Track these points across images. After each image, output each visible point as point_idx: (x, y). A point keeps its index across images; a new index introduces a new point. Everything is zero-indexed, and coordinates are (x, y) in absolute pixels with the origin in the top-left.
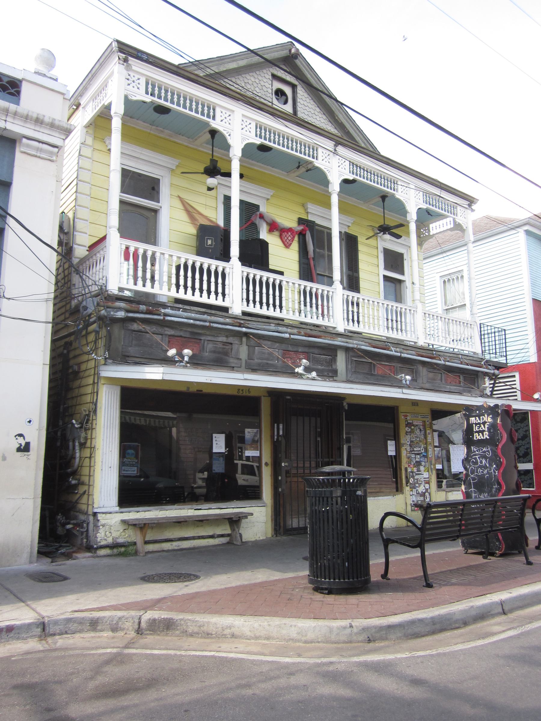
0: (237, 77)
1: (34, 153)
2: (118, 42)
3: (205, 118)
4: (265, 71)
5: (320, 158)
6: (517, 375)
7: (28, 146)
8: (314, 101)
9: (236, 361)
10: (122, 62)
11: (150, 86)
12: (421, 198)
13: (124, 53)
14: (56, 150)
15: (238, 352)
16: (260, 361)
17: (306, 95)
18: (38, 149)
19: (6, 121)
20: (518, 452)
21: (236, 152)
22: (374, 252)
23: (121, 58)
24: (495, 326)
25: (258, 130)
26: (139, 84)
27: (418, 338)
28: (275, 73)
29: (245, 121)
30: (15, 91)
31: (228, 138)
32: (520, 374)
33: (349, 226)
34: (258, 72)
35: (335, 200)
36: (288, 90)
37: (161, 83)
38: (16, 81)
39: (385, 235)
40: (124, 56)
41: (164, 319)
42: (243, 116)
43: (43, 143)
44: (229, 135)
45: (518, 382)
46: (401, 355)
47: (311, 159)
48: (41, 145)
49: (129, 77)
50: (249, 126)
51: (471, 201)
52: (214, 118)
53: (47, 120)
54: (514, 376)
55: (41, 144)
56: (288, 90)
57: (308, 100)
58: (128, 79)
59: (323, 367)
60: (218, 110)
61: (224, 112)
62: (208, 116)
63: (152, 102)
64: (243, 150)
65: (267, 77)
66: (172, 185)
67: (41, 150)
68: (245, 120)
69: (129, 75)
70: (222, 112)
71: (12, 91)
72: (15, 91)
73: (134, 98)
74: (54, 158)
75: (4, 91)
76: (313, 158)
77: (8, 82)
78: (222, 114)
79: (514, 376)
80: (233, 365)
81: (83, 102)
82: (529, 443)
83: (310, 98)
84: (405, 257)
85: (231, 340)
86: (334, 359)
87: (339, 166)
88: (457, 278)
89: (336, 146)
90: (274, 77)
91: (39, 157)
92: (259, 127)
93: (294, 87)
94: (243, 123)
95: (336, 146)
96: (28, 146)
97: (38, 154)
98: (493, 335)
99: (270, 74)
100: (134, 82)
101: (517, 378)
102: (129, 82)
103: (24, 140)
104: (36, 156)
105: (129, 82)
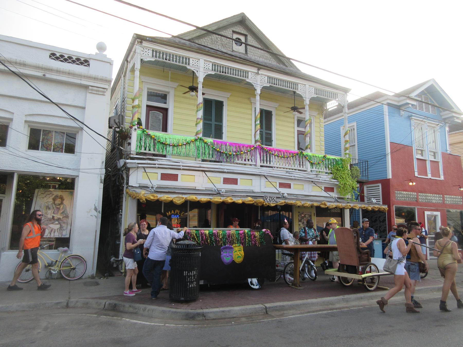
0: (212, 35)
1: (96, 92)
2: (136, 34)
3: (184, 65)
4: (228, 30)
5: (250, 77)
6: (380, 185)
7: (92, 90)
8: (258, 42)
10: (139, 43)
11: (154, 53)
12: (313, 92)
13: (140, 39)
14: (106, 90)
17: (253, 39)
18: (97, 91)
19: (81, 80)
20: (380, 229)
21: (201, 79)
22: (292, 120)
23: (138, 41)
25: (214, 67)
26: (149, 52)
27: (307, 168)
28: (235, 30)
29: (206, 63)
30: (87, 64)
31: (196, 73)
33: (276, 108)
34: (224, 31)
37: (160, 51)
38: (87, 59)
39: (294, 112)
40: (140, 40)
42: (205, 60)
43: (99, 87)
44: (197, 72)
45: (381, 190)
47: (244, 78)
48: (98, 89)
49: (144, 50)
50: (208, 66)
51: (346, 91)
52: (189, 64)
53: (99, 77)
54: (379, 186)
55: (98, 88)
56: (243, 39)
58: (143, 51)
60: (191, 60)
61: (194, 60)
62: (186, 64)
63: (155, 61)
64: (205, 79)
65: (230, 33)
66: (175, 96)
67: (99, 91)
69: (144, 49)
70: (193, 60)
71: (86, 64)
72: (87, 64)
73: (146, 60)
75: (82, 65)
76: (246, 77)
77: (83, 61)
78: (193, 62)
81: (129, 60)
82: (386, 224)
83: (255, 41)
87: (261, 80)
88: (352, 130)
89: (259, 70)
90: (234, 32)
91: (98, 94)
92: (214, 65)
93: (246, 36)
94: (205, 64)
95: (259, 70)
96: (92, 90)
97: (98, 93)
98: (362, 164)
99: (232, 31)
100: (146, 52)
101: (380, 187)
102: (144, 52)
103: (90, 87)
104: (96, 94)
105: (144, 52)
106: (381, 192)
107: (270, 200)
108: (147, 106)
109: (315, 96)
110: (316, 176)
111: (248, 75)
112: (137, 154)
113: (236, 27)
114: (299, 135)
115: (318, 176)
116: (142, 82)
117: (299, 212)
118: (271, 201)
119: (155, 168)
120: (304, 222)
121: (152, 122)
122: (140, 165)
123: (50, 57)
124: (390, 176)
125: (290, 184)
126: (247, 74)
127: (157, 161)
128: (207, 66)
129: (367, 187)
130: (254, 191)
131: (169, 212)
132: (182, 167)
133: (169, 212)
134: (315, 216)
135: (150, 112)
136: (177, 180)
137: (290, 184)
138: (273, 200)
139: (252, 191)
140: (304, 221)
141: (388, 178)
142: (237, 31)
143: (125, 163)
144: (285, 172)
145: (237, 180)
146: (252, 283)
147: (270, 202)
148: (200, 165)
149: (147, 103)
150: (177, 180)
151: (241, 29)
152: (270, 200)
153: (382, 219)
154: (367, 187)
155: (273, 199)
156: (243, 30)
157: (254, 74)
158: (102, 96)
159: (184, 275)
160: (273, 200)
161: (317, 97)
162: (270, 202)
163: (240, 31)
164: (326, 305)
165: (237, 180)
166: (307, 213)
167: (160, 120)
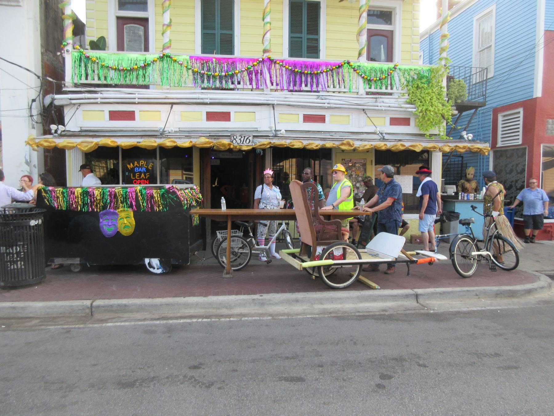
6: (521, 110)
24: (460, 66)
32: (524, 110)
45: (521, 119)
79: (519, 113)
91: (11, 6)
101: (521, 115)
104: (9, 5)
106: (521, 122)
107: (242, 139)
108: (118, 18)
110: (375, 100)
112: (76, 85)
114: (372, 38)
115: (378, 100)
117: (342, 160)
118: (244, 142)
119: (97, 103)
120: (352, 175)
121: (129, 41)
122: (73, 102)
124: (538, 93)
125: (325, 115)
127: (101, 93)
129: (505, 116)
130: (258, 129)
131: (131, 164)
132: (137, 101)
133: (131, 164)
134: (372, 164)
135: (125, 26)
136: (133, 119)
137: (325, 115)
138: (248, 141)
139: (256, 130)
140: (353, 173)
141: (534, 97)
143: (53, 99)
144: (316, 97)
145: (228, 114)
146: (151, 266)
147: (243, 143)
148: (167, 95)
149: (148, 14)
150: (133, 119)
152: (242, 139)
153: (519, 169)
154: (505, 116)
155: (247, 138)
159: (2, 252)
160: (248, 141)
162: (243, 143)
164: (214, 308)
165: (228, 114)
166: (358, 161)
167: (140, 36)
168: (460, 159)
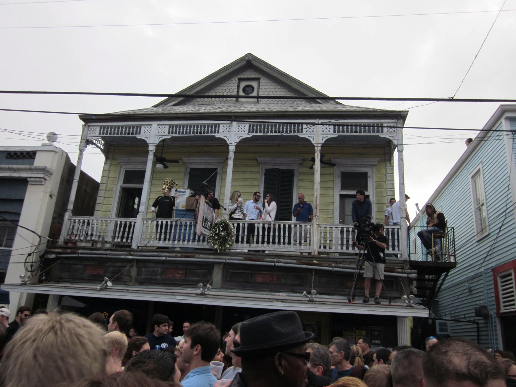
9: (127, 278)
15: (129, 271)
16: (145, 277)
17: (268, 81)
25: (171, 129)
35: (231, 156)
36: (254, 84)
41: (78, 256)
46: (275, 264)
56: (254, 84)
57: (269, 84)
59: (199, 279)
68: (161, 127)
74: (43, 183)
80: (125, 280)
84: (369, 174)
85: (124, 264)
86: (210, 272)
93: (258, 79)
96: (31, 181)
109: (336, 135)
111: (219, 129)
113: (244, 73)
116: (119, 163)
123: (7, 156)
126: (217, 128)
128: (147, 130)
142: (245, 76)
151: (251, 73)
156: (255, 73)
157: (228, 125)
158: (40, 186)
161: (339, 136)
163: (249, 76)
168: (476, 326)
